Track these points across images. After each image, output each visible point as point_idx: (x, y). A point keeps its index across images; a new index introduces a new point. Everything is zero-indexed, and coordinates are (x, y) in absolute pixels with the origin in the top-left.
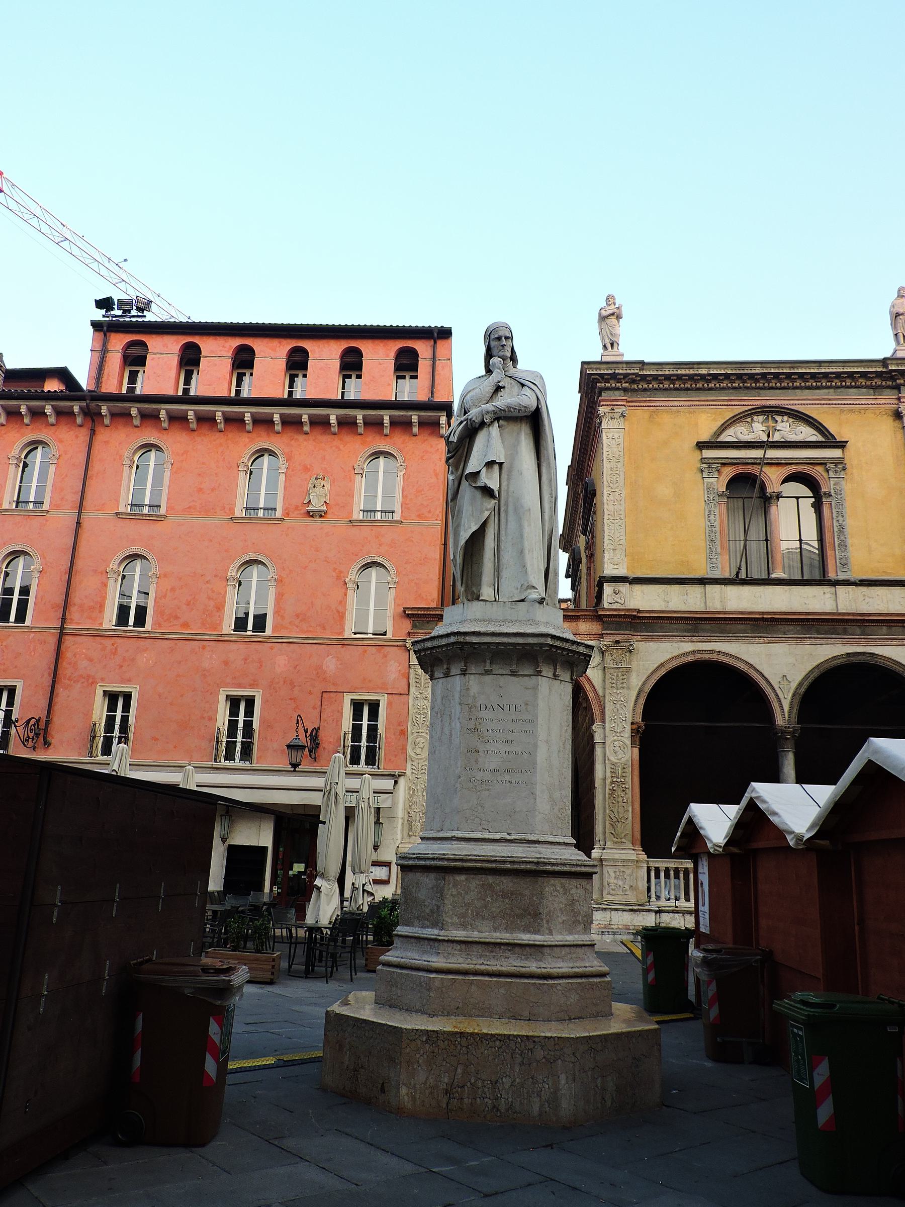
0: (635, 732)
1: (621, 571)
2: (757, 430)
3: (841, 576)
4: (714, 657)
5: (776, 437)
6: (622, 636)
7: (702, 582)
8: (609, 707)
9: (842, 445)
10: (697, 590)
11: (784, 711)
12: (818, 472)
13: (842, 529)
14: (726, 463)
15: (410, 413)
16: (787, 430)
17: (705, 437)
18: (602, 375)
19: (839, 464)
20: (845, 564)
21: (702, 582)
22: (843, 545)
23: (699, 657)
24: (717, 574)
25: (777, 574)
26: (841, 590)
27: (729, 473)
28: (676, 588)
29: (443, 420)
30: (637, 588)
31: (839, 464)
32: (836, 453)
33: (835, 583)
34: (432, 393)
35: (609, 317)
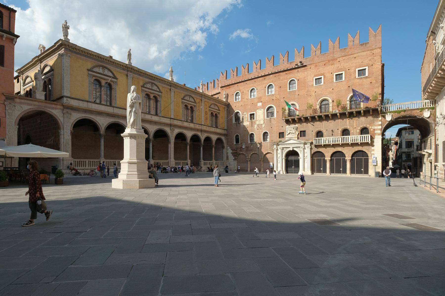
0: (71, 132)
1: (69, 95)
2: (100, 70)
3: (115, 106)
4: (89, 118)
5: (105, 73)
6: (69, 111)
7: (88, 101)
8: (65, 126)
9: (117, 79)
10: (86, 103)
11: (102, 130)
12: (112, 83)
13: (116, 96)
14: (94, 76)
15: (4, 34)
16: (106, 72)
17: (89, 68)
18: (65, 44)
19: (116, 82)
20: (116, 104)
21: (88, 101)
22: (116, 100)
23: (86, 118)
24: (90, 100)
25: (103, 103)
26: (115, 108)
27: (94, 78)
28: (81, 102)
29: (15, 40)
30: (72, 100)
31: (116, 82)
32: (116, 80)
33: (114, 107)
34: (10, 29)
35: (66, 28)
